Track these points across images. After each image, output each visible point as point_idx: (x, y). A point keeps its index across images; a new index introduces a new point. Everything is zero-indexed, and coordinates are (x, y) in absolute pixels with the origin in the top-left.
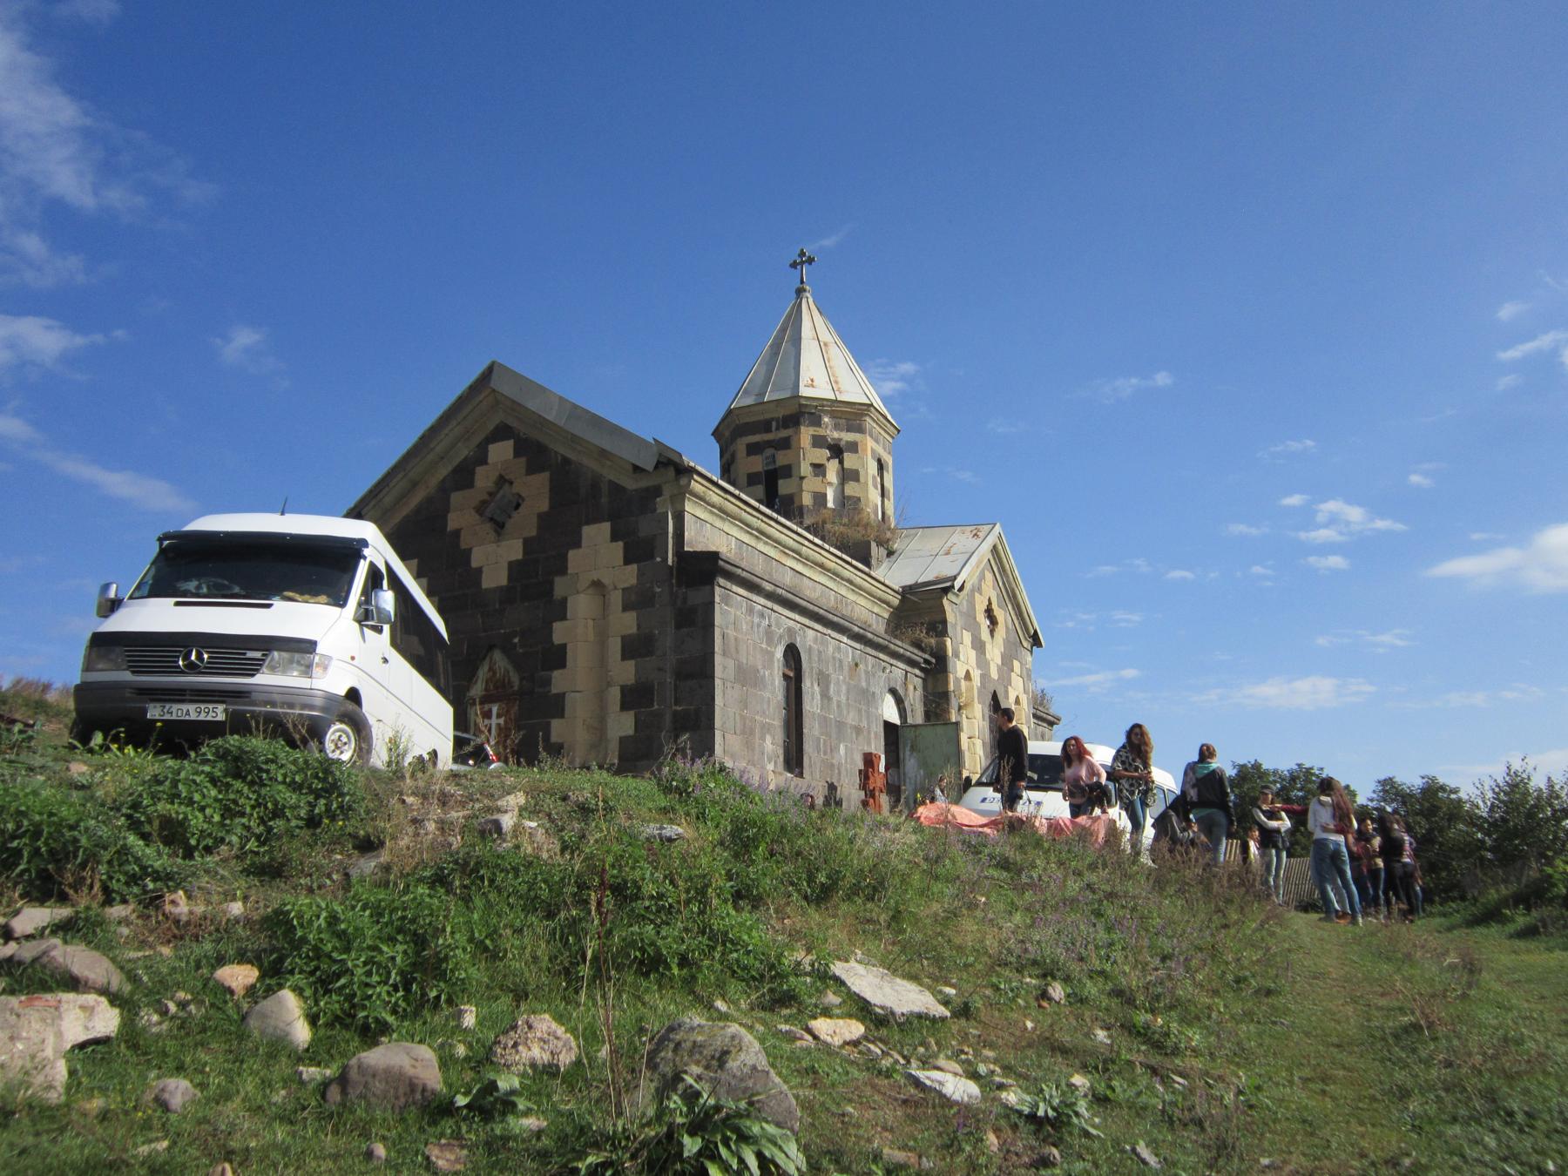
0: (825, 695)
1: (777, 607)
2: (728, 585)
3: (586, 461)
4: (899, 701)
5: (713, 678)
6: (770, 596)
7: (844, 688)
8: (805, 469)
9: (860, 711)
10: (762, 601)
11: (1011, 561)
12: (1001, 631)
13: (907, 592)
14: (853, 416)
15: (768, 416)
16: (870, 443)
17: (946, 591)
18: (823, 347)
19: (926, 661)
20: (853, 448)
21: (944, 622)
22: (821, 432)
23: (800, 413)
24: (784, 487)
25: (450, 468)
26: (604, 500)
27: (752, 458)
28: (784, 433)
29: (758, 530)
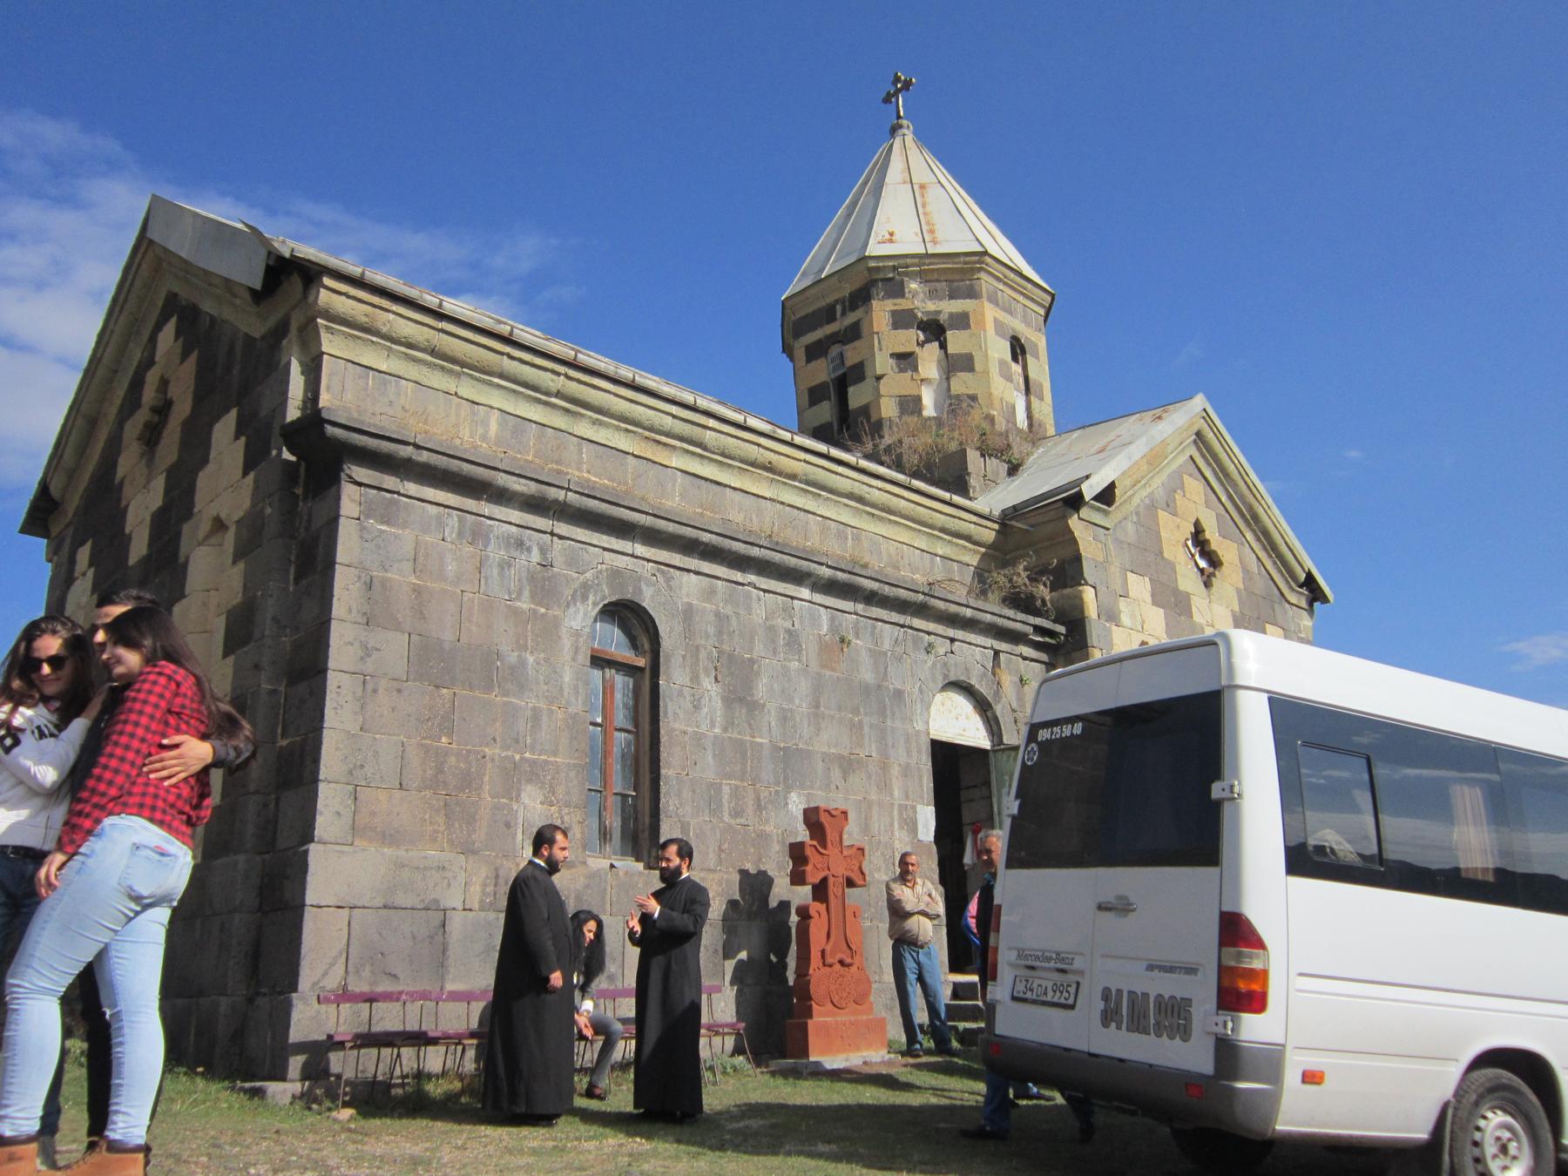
0: (740, 698)
1: (563, 528)
2: (390, 481)
3: (227, 314)
4: (983, 706)
5: (324, 671)
6: (536, 505)
7: (804, 686)
8: (882, 363)
9: (856, 728)
10: (516, 515)
11: (1236, 457)
12: (1230, 579)
13: (1008, 520)
14: (960, 273)
15: (830, 300)
16: (990, 313)
17: (1075, 502)
18: (918, 191)
19: (1039, 630)
20: (962, 321)
21: (1077, 559)
22: (903, 304)
23: (871, 281)
24: (857, 396)
25: (126, 385)
26: (236, 371)
27: (813, 364)
28: (851, 318)
29: (558, 395)
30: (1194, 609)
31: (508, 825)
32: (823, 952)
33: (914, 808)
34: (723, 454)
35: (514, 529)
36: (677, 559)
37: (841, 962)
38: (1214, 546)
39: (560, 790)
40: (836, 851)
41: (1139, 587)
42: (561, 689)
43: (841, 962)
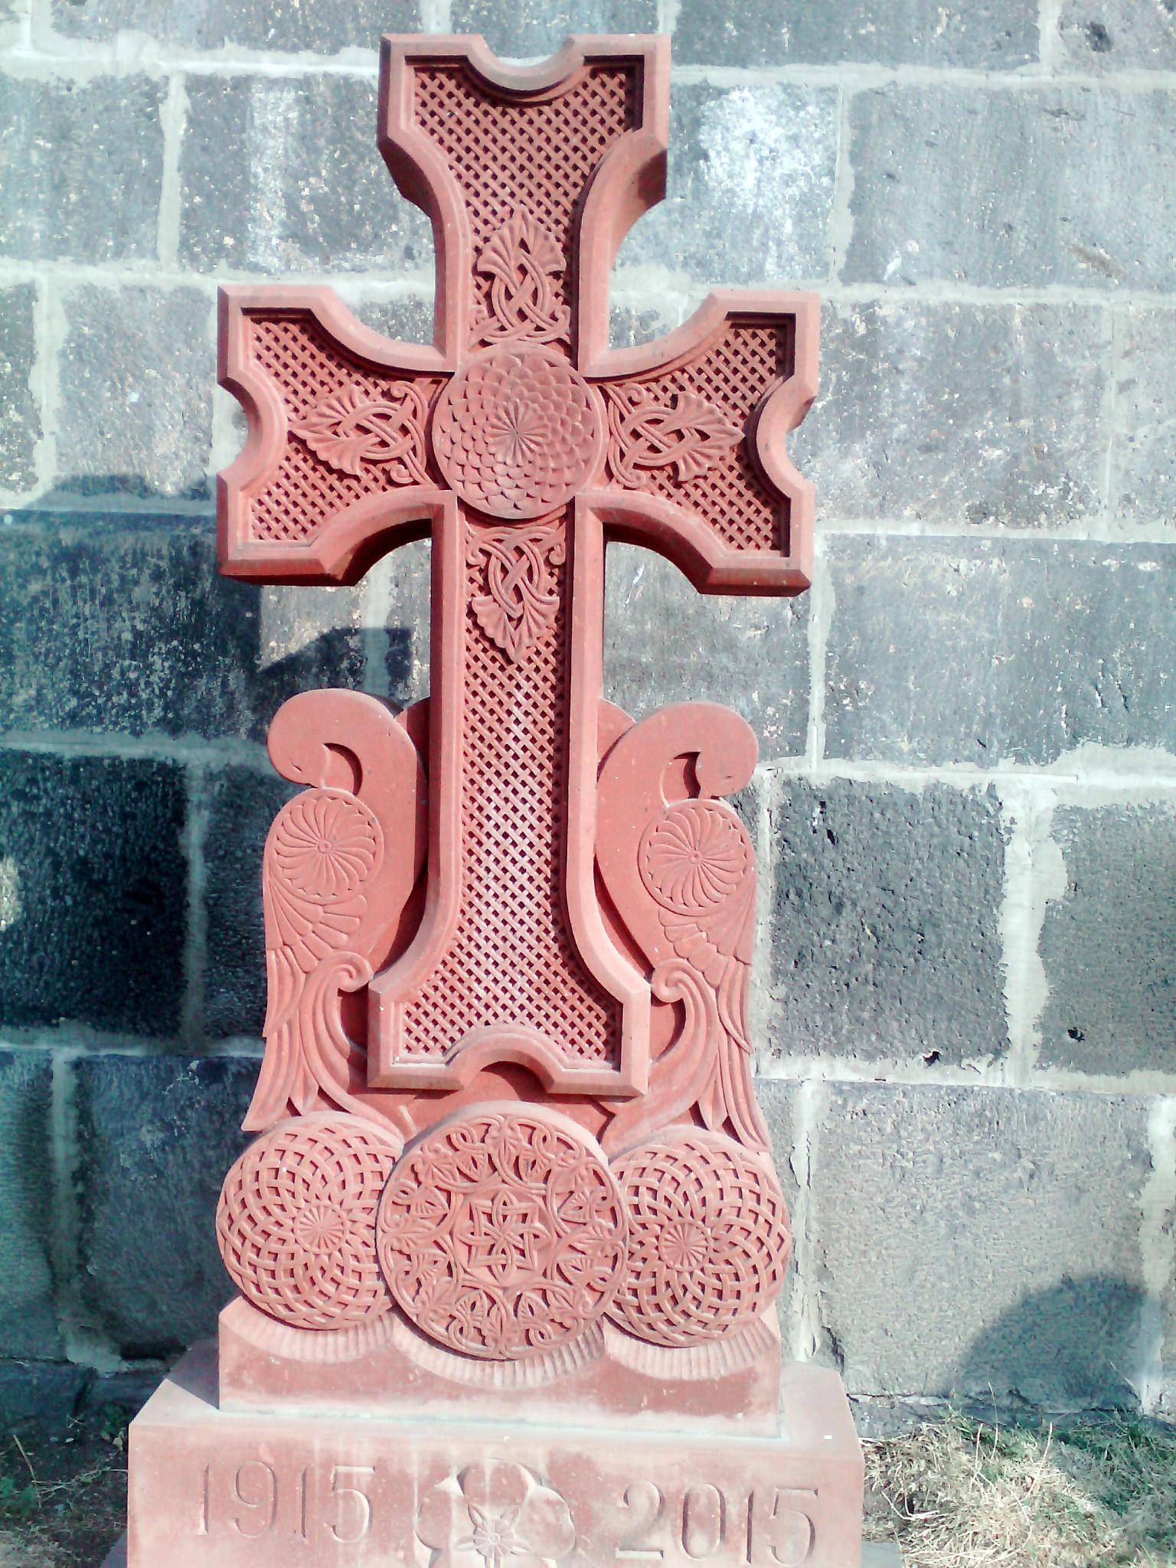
32: (359, 1008)
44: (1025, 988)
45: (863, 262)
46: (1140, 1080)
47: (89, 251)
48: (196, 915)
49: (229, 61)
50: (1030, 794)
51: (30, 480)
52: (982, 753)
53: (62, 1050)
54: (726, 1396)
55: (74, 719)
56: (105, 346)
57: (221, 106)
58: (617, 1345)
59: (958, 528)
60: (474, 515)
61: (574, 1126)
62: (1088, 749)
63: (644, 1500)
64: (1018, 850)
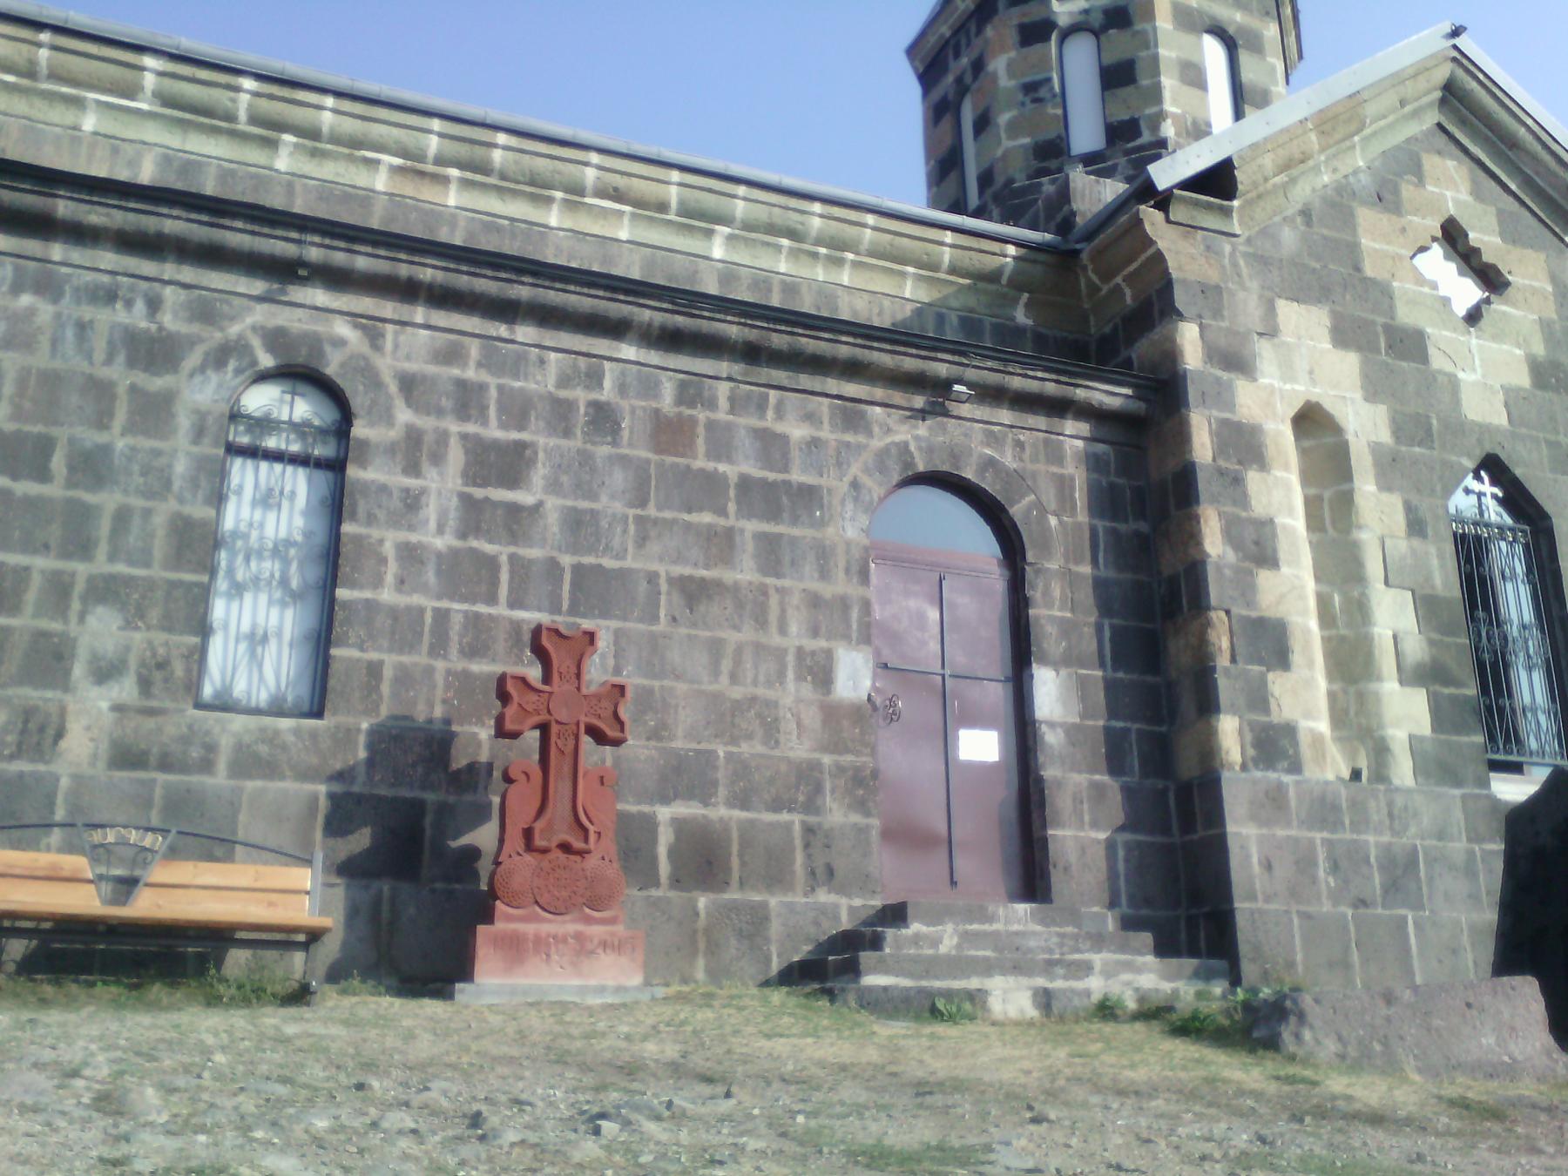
7: (619, 479)
10: (108, 258)
21: (1167, 285)
30: (1432, 351)
31: (59, 657)
32: (528, 834)
33: (829, 655)
34: (532, 183)
35: (106, 279)
36: (388, 308)
37: (565, 847)
38: (1487, 257)
39: (154, 615)
40: (569, 687)
41: (1304, 324)
42: (167, 484)
43: (565, 847)
44: (664, 868)
45: (617, 671)
46: (695, 894)
47: (401, 651)
48: (427, 844)
49: (444, 604)
50: (664, 813)
51: (378, 715)
52: (651, 803)
53: (386, 887)
54: (612, 921)
55: (393, 785)
56: (404, 678)
57: (442, 616)
58: (587, 910)
59: (643, 742)
60: (558, 722)
61: (578, 858)
62: (678, 802)
63: (596, 941)
64: (661, 829)
